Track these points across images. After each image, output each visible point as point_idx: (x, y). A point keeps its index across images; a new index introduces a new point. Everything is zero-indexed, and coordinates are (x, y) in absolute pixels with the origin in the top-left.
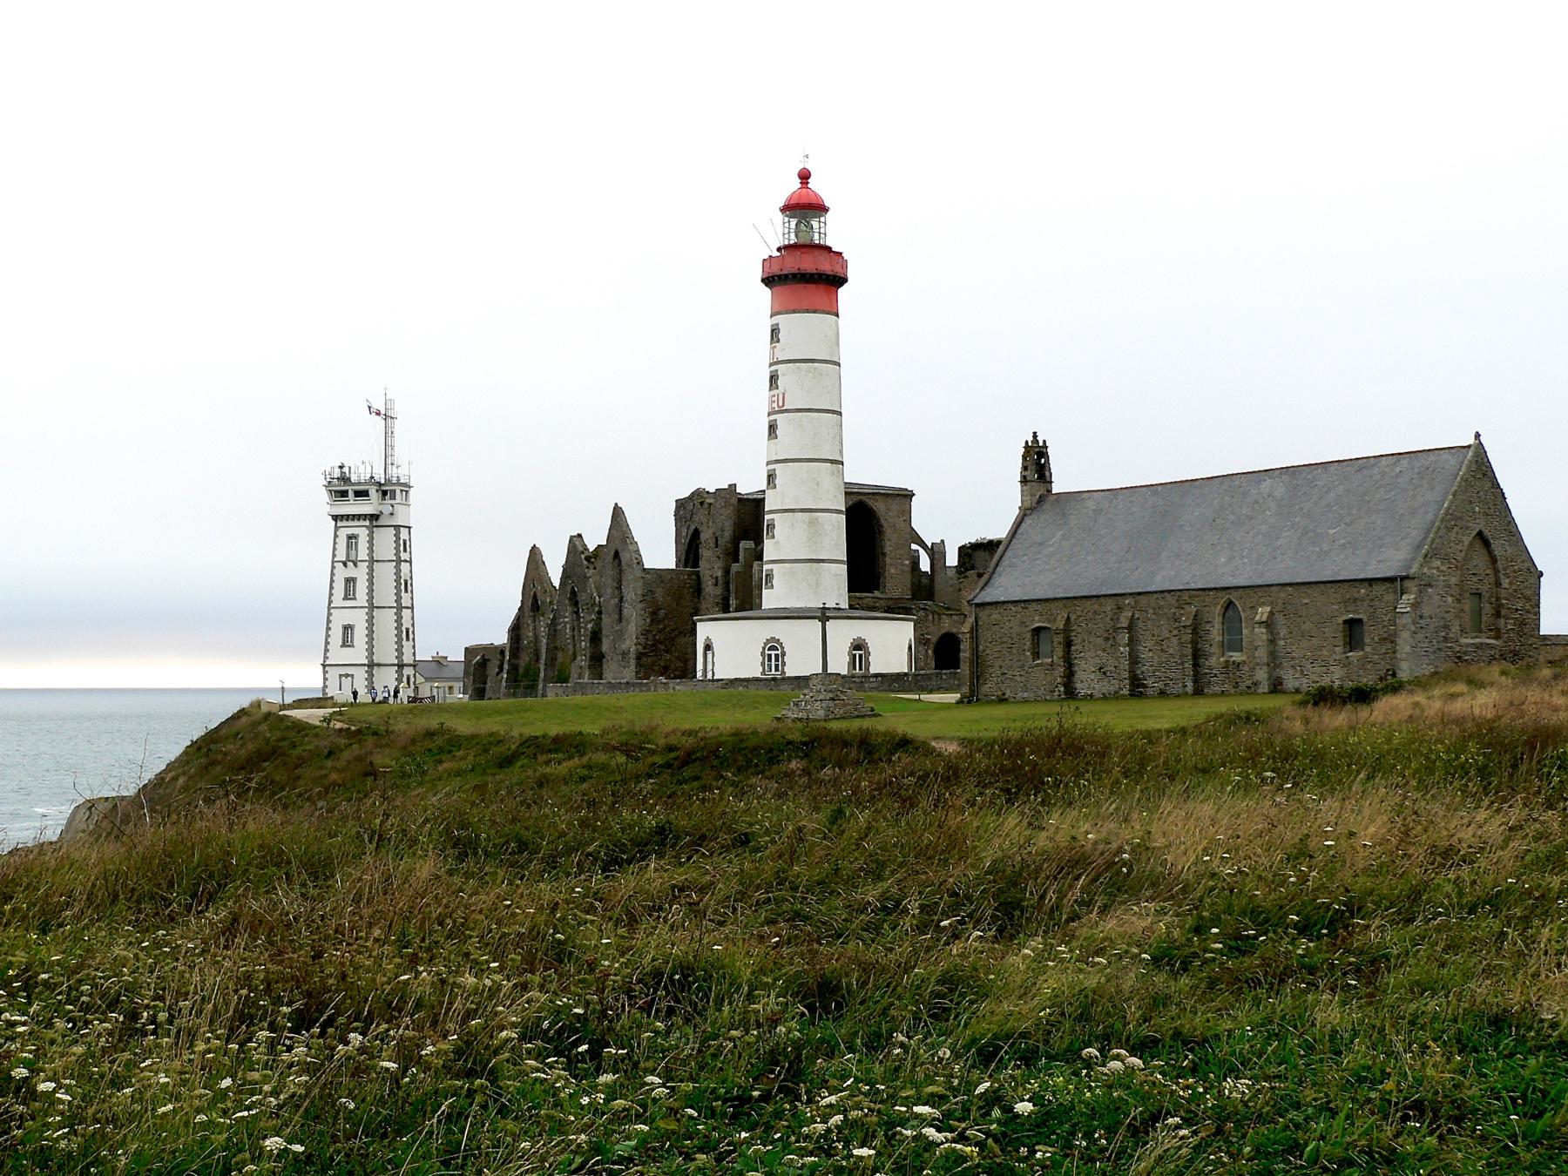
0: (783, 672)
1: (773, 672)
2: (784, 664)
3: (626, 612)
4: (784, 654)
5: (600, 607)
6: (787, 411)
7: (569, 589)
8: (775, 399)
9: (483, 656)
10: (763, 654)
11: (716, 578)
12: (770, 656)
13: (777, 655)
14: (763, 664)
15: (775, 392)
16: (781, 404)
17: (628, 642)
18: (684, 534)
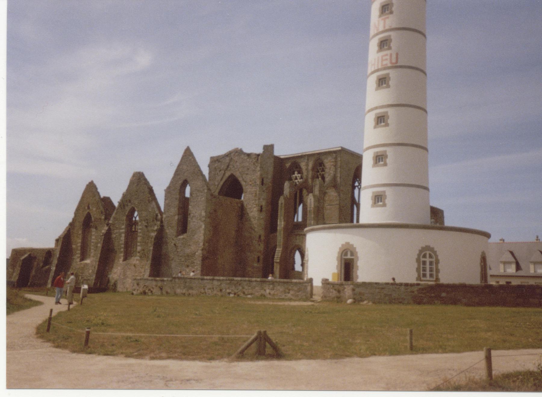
0: (437, 279)
1: (428, 278)
2: (438, 271)
3: (192, 224)
4: (437, 262)
5: (162, 222)
6: (401, 67)
7: (128, 209)
8: (388, 57)
9: (30, 255)
10: (418, 260)
11: (261, 207)
12: (424, 263)
13: (431, 263)
14: (418, 270)
15: (388, 52)
16: (394, 61)
17: (193, 248)
18: (219, 178)
